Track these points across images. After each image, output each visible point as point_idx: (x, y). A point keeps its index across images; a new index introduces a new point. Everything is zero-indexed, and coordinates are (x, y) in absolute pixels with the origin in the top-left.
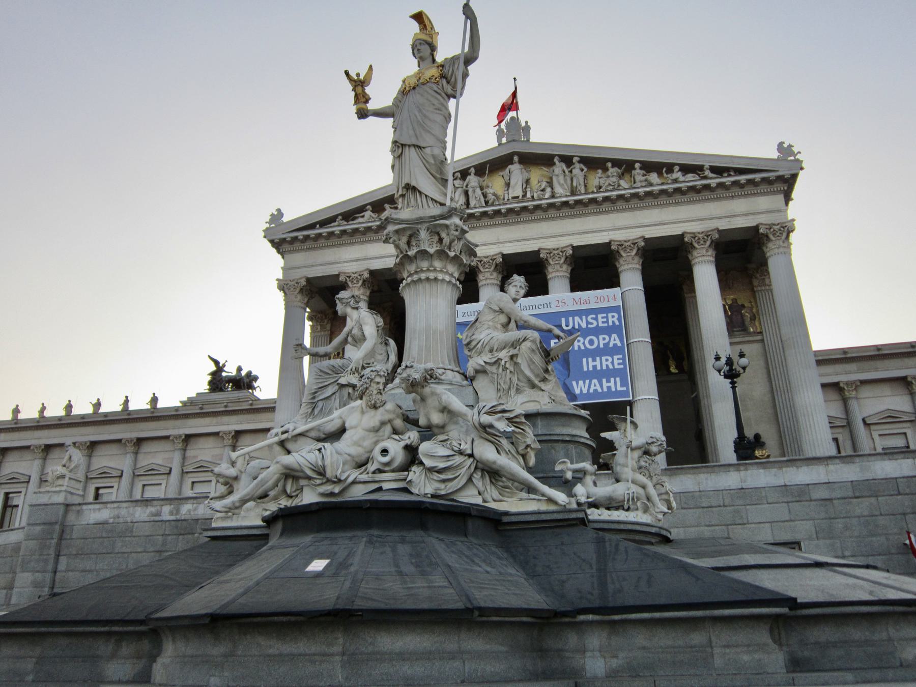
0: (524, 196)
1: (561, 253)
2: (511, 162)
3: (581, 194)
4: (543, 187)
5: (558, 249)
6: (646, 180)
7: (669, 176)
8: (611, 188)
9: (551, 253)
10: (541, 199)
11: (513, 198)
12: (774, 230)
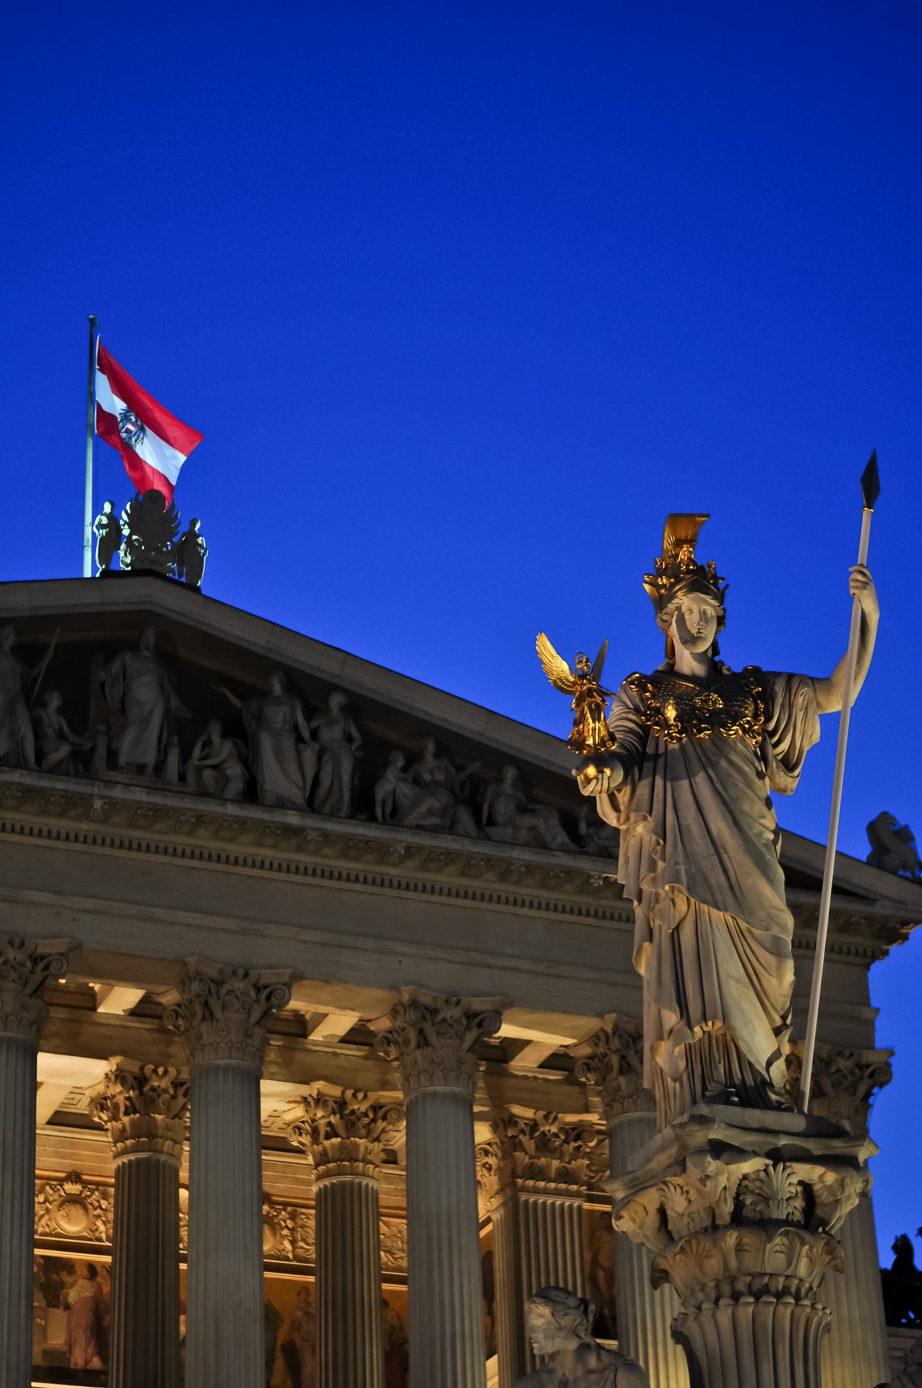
0: (160, 767)
1: (253, 994)
2: (133, 646)
3: (333, 815)
4: (223, 756)
5: (246, 975)
6: (532, 829)
7: (592, 830)
8: (431, 821)
9: (222, 983)
10: (224, 801)
11: (140, 769)
12: (839, 1071)
